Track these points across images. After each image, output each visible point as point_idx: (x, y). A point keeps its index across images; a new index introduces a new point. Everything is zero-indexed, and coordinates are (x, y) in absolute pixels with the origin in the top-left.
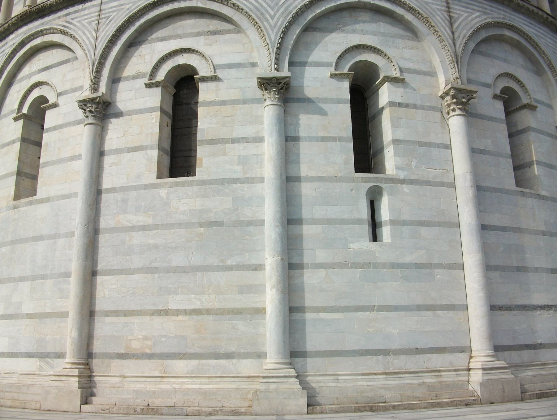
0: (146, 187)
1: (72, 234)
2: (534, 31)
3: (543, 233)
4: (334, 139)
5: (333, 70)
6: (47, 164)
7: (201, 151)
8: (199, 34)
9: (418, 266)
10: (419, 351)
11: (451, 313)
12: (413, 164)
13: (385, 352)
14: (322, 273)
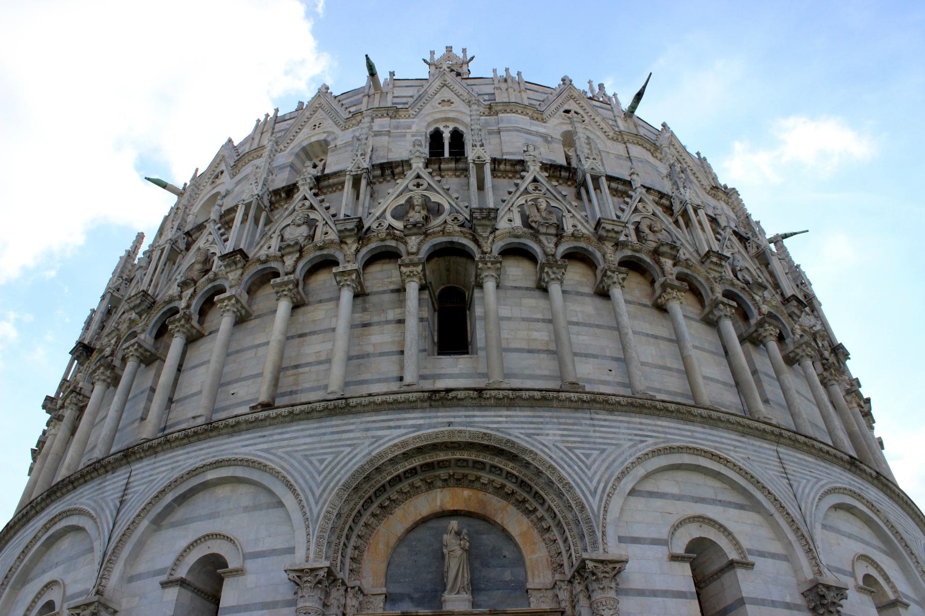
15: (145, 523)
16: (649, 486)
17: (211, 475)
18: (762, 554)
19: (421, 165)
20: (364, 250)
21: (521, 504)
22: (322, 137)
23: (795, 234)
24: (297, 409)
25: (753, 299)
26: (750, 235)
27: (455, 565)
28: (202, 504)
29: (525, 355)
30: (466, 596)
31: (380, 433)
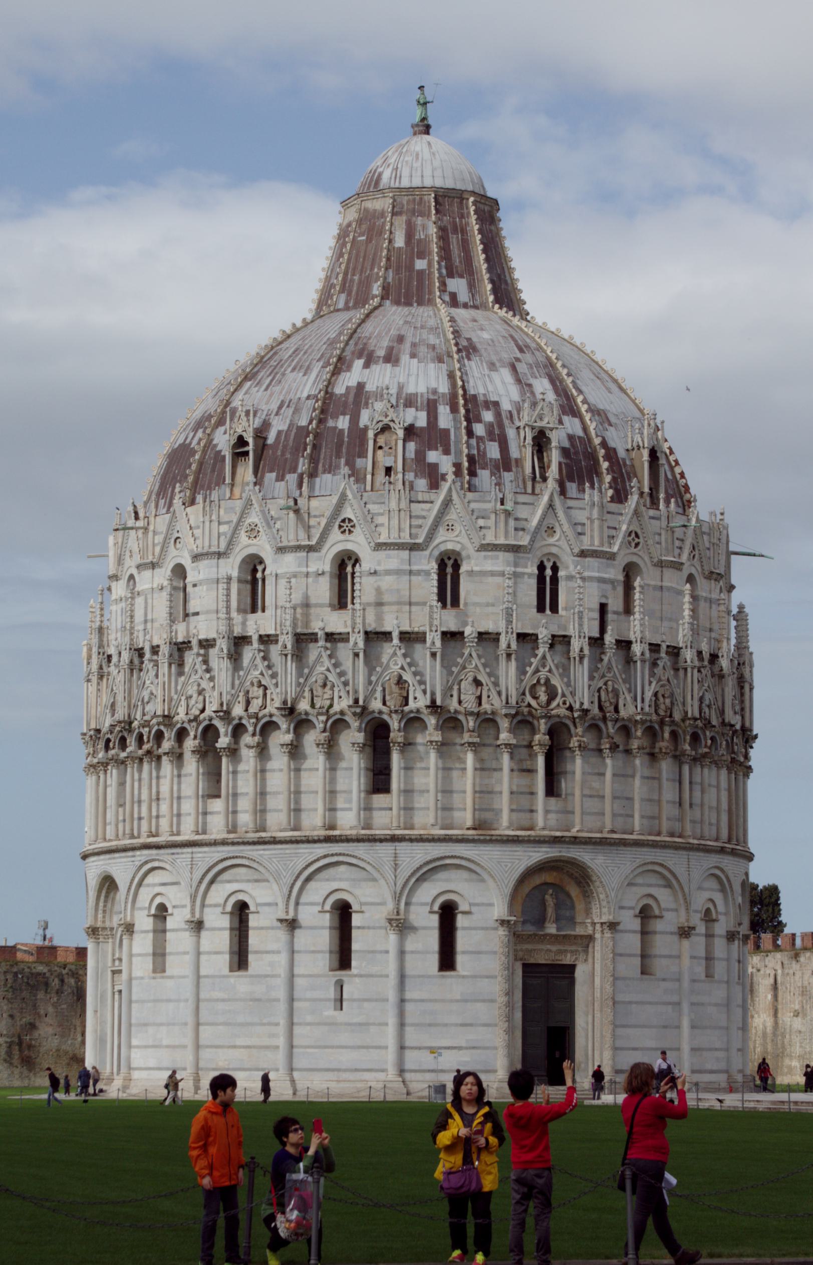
0: (224, 976)
1: (187, 1000)
2: (477, 852)
3: (457, 1001)
4: (319, 952)
5: (320, 908)
6: (171, 954)
7: (251, 957)
8: (249, 881)
9: (360, 1024)
10: (356, 1070)
11: (378, 1051)
12: (363, 965)
13: (339, 1070)
14: (309, 1028)
15: (413, 880)
16: (633, 881)
17: (448, 861)
18: (668, 910)
19: (547, 649)
20: (515, 721)
21: (579, 884)
22: (458, 548)
23: (762, 556)
24: (494, 838)
25: (705, 735)
26: (720, 655)
27: (550, 911)
28: (442, 875)
29: (589, 799)
30: (555, 925)
31: (531, 854)
